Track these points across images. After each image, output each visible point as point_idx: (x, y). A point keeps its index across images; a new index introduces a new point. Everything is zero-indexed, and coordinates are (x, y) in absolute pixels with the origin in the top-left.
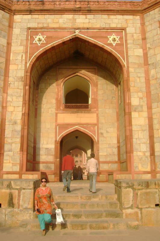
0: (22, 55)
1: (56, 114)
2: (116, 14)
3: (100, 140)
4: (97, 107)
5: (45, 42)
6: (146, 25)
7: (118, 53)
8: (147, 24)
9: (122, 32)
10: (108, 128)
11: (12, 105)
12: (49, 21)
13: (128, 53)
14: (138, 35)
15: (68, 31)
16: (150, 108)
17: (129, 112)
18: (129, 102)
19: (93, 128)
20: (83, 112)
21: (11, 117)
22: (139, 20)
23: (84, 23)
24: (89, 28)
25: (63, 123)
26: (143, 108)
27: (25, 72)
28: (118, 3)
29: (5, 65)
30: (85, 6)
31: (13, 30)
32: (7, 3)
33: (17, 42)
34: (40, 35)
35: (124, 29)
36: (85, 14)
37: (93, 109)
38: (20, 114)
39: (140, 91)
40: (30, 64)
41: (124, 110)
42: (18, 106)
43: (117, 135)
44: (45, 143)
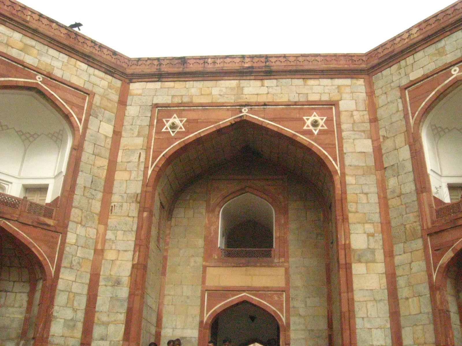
0: (140, 153)
1: (205, 268)
2: (318, 76)
3: (291, 322)
4: (285, 255)
5: (184, 130)
6: (376, 95)
7: (323, 148)
8: (378, 92)
9: (332, 108)
10: (309, 297)
11: (114, 247)
13: (342, 147)
14: (362, 113)
15: (228, 110)
16: (389, 255)
17: (346, 264)
18: (347, 242)
19: (279, 297)
20: (258, 265)
21: (111, 271)
22: (364, 87)
23: (257, 94)
24: (267, 104)
25: (217, 287)
26: (376, 254)
27: (143, 185)
28: (322, 58)
29: (108, 170)
31: (126, 109)
32: (118, 63)
33: (133, 130)
34: (175, 118)
35: (334, 104)
36: (261, 78)
37: (279, 258)
38: (129, 266)
39: (370, 221)
40: (153, 170)
42: (125, 249)
43: (328, 311)
44: (179, 327)
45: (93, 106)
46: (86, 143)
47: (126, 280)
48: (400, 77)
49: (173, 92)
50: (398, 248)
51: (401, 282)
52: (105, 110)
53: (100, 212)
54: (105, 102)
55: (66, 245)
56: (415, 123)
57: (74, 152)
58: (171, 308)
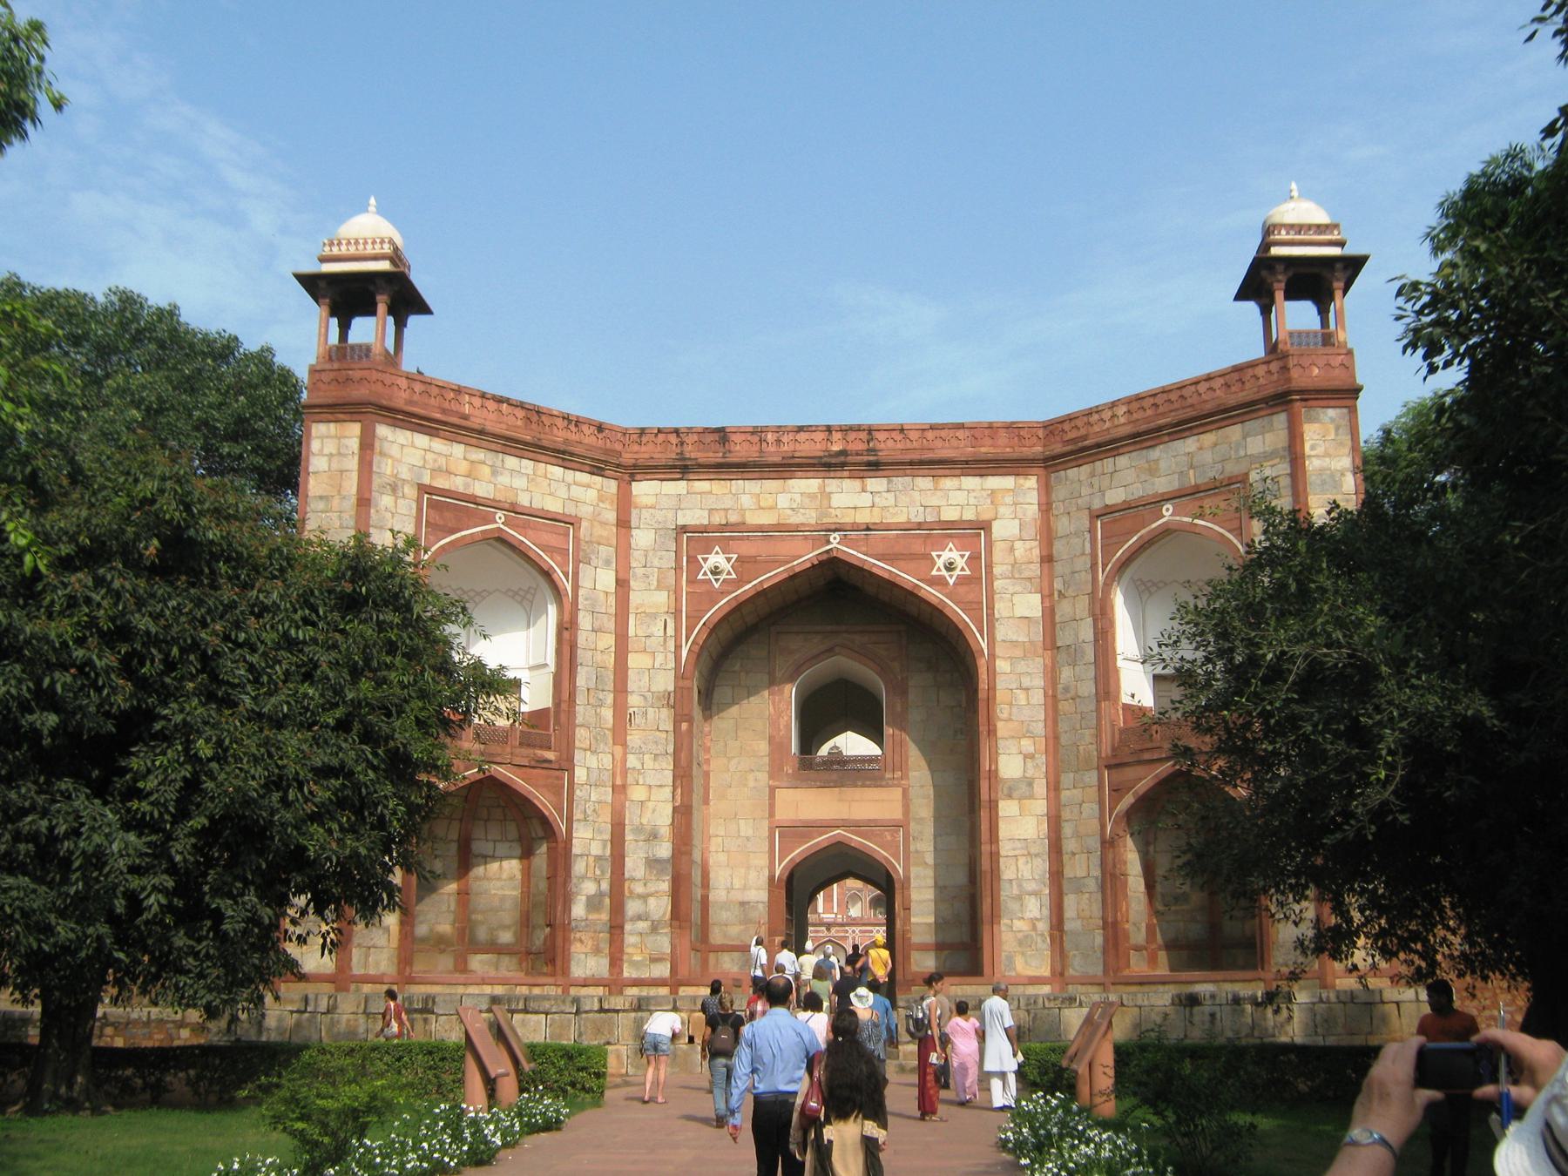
2: (958, 472)
8: (1058, 508)
12: (746, 501)
14: (1028, 544)
16: (1054, 787)
22: (1035, 493)
28: (967, 433)
30: (862, 447)
35: (984, 526)
38: (668, 810)
45: (583, 545)
46: (581, 614)
47: (665, 831)
48: (1089, 491)
49: (711, 502)
50: (1067, 779)
51: (1067, 830)
54: (600, 532)
56: (1105, 584)
57: (566, 634)
58: (722, 857)
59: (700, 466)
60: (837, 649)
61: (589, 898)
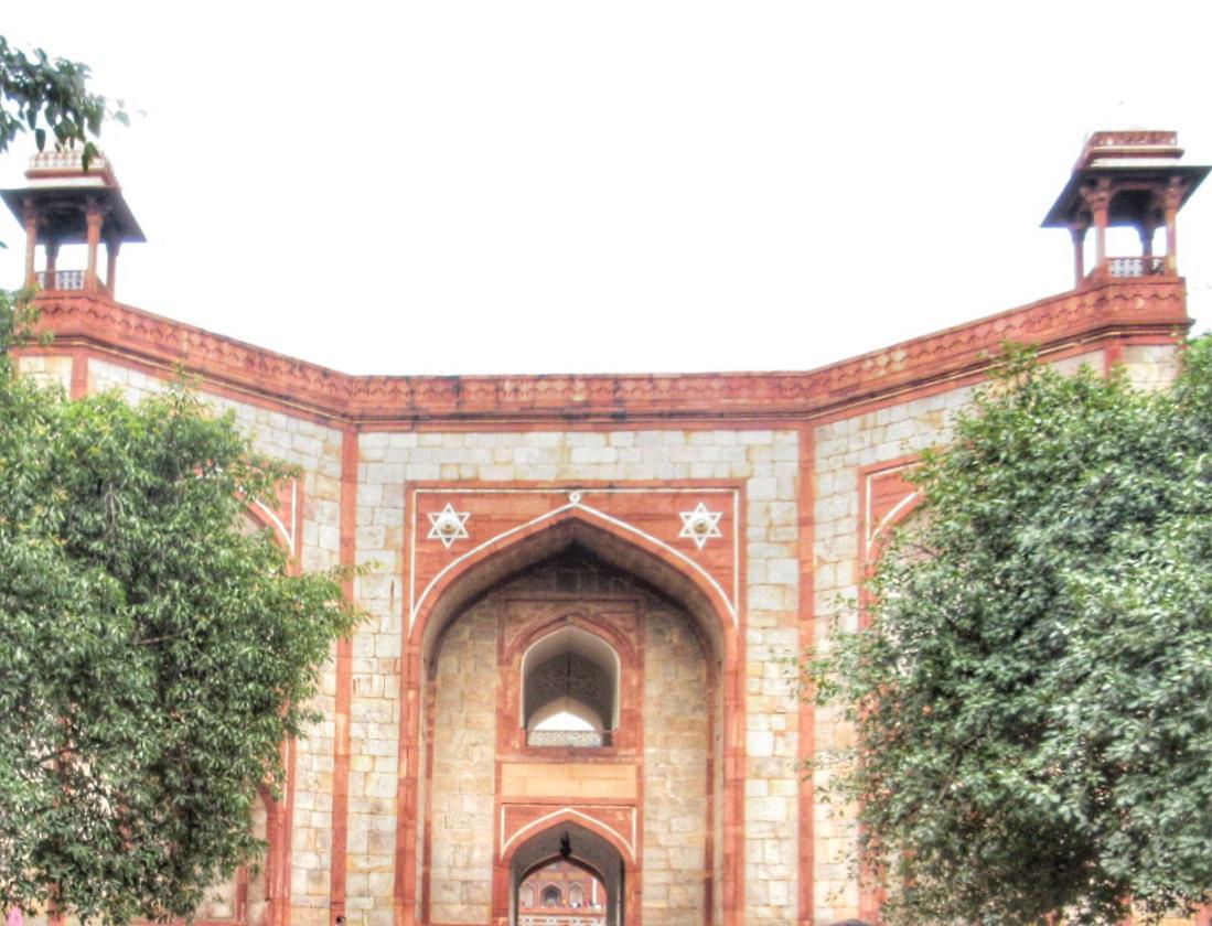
4: (638, 744)
5: (466, 536)
7: (713, 576)
9: (730, 495)
12: (480, 455)
17: (736, 780)
19: (624, 815)
20: (591, 759)
21: (364, 788)
23: (598, 464)
30: (605, 397)
35: (738, 485)
36: (605, 427)
38: (393, 782)
40: (418, 615)
41: (724, 769)
52: (323, 498)
53: (337, 692)
55: (298, 755)
59: (433, 417)
60: (570, 619)
61: (310, 872)
